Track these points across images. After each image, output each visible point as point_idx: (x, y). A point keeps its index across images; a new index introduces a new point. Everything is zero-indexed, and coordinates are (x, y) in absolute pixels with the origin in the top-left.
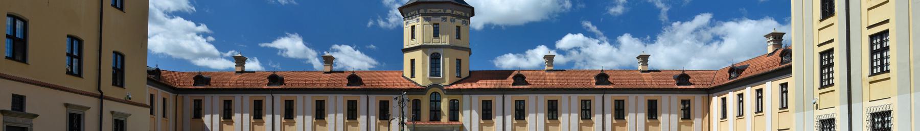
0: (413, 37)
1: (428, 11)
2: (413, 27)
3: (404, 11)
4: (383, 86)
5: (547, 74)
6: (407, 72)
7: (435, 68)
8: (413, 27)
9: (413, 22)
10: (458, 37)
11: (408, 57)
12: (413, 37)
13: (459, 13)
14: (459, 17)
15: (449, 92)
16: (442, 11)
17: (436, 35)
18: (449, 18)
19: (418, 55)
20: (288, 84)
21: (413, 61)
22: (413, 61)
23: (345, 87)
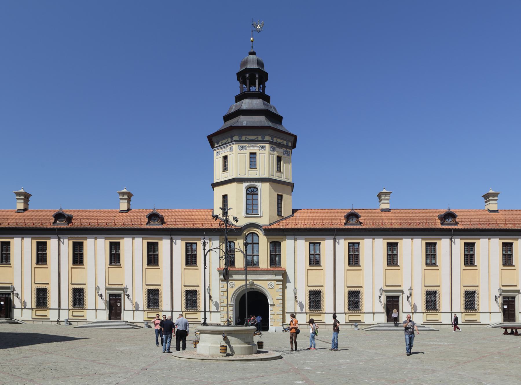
0: (225, 169)
1: (244, 138)
2: (225, 158)
3: (214, 139)
4: (190, 226)
5: (383, 213)
6: (218, 212)
7: (252, 206)
8: (225, 158)
9: (224, 152)
10: (279, 169)
11: (219, 192)
12: (225, 169)
13: (280, 141)
14: (280, 145)
15: (268, 232)
16: (260, 138)
17: (253, 165)
18: (267, 146)
19: (230, 189)
20: (76, 224)
21: (225, 197)
22: (225, 197)
23: (144, 226)
